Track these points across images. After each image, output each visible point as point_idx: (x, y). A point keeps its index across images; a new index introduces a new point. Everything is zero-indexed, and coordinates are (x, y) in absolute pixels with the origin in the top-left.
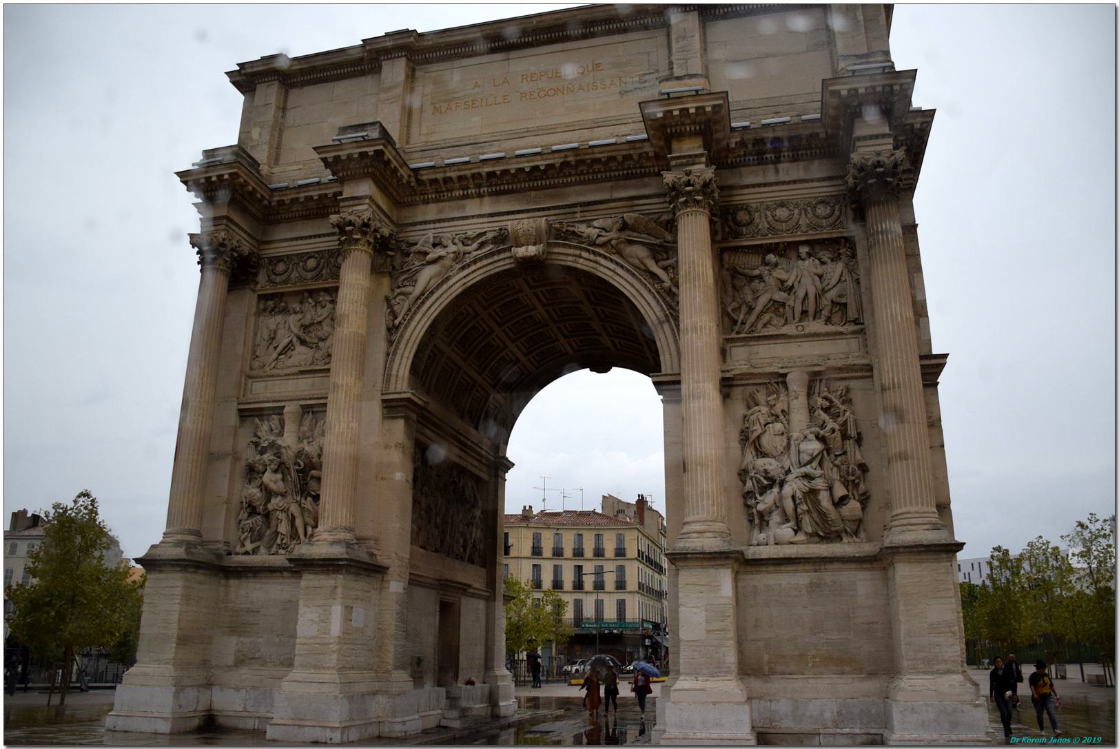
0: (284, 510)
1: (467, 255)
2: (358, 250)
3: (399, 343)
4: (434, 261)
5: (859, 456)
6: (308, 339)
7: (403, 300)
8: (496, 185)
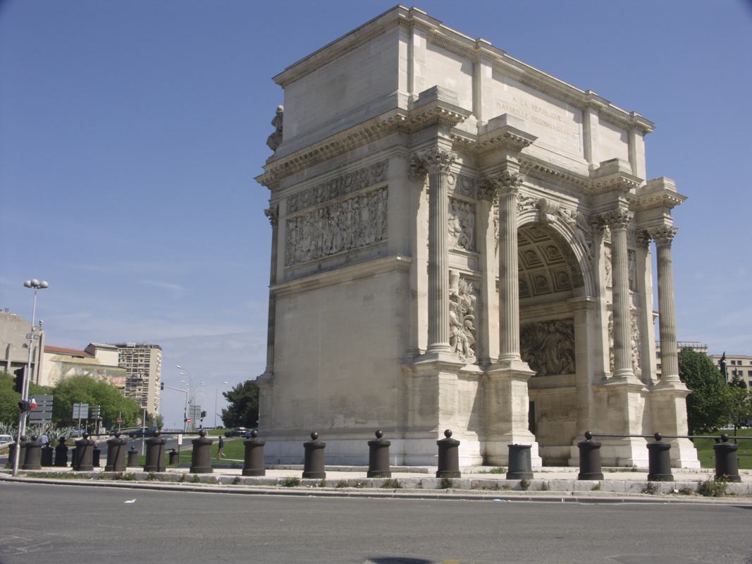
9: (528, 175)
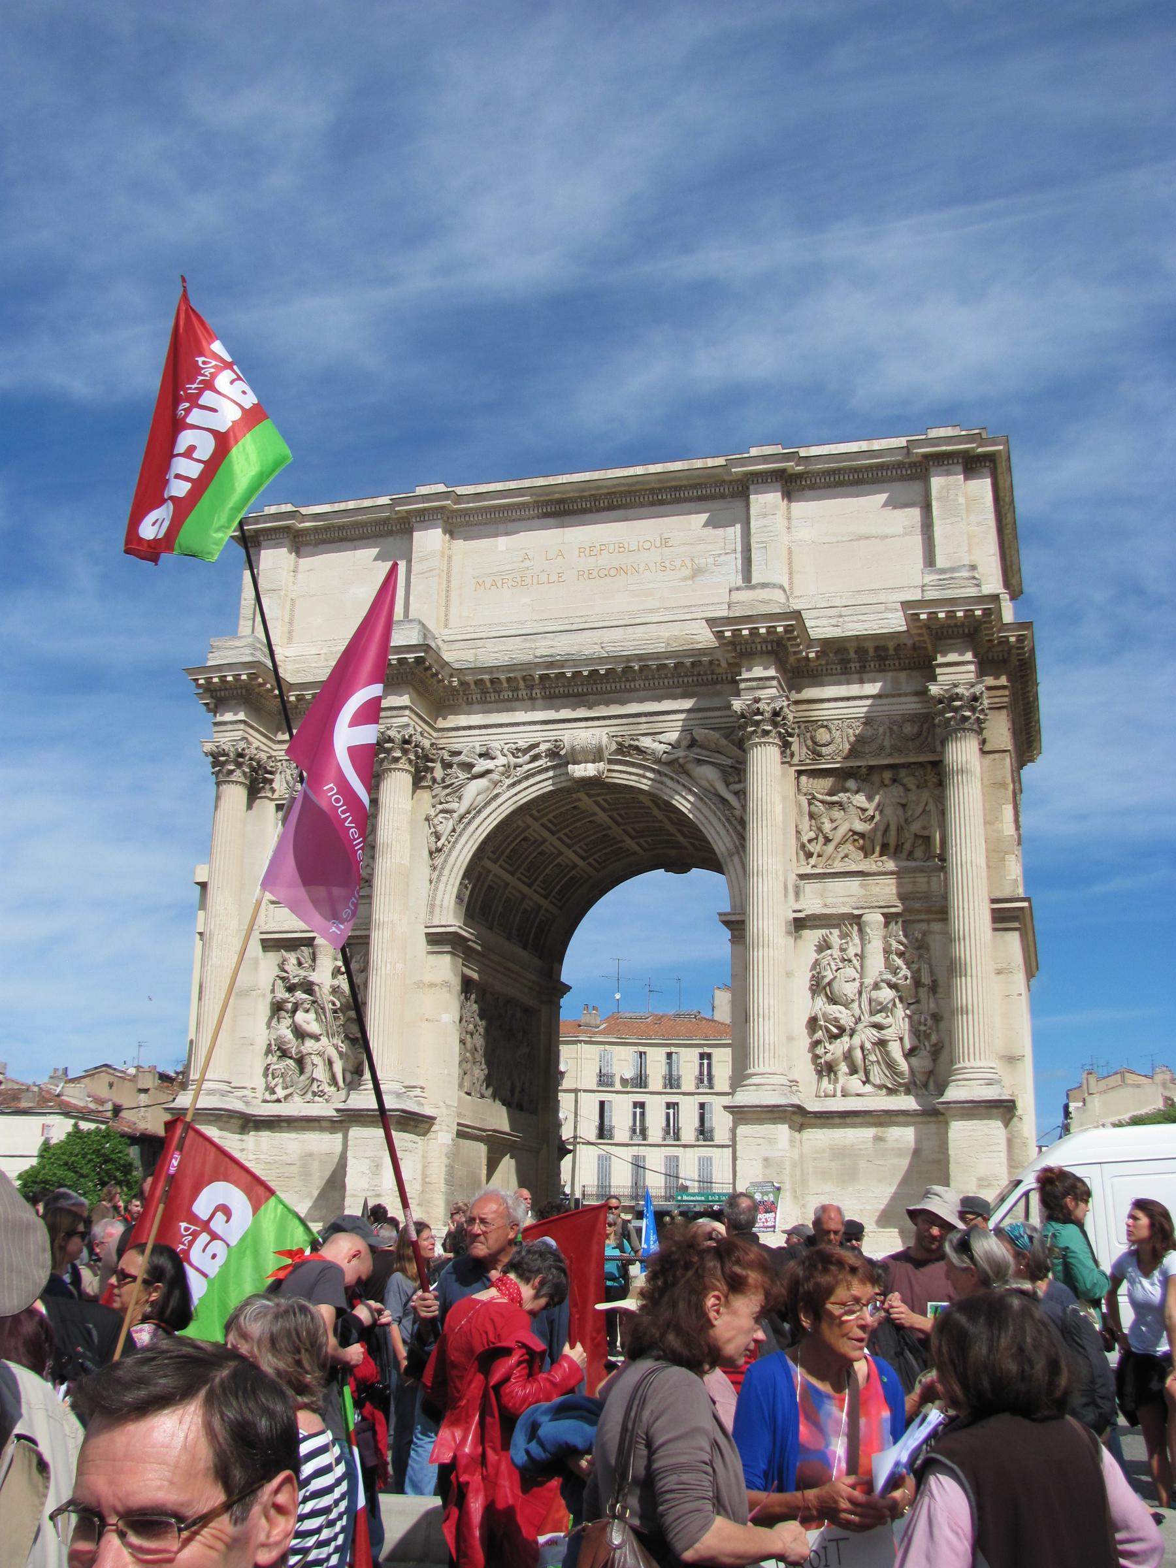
0: (320, 1054)
1: (518, 769)
2: (399, 769)
3: (443, 868)
4: (482, 775)
5: (932, 1005)
7: (445, 818)
8: (550, 688)
9: (543, 698)
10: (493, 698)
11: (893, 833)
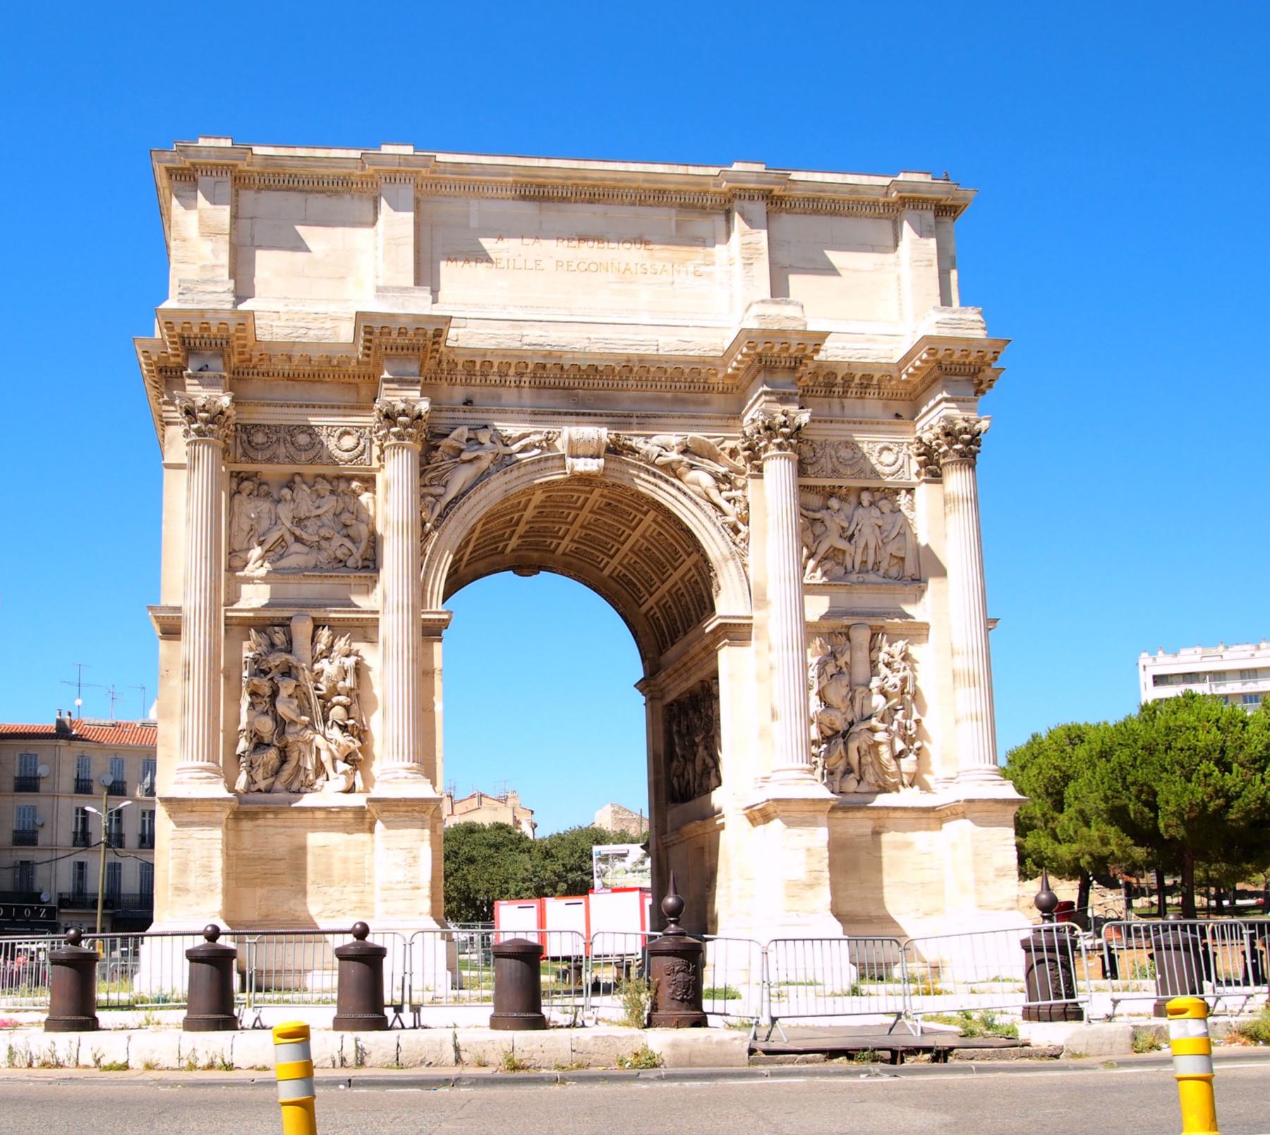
1: (507, 458)
4: (470, 461)
6: (305, 536)
9: (530, 387)
10: (478, 381)
11: (871, 552)
